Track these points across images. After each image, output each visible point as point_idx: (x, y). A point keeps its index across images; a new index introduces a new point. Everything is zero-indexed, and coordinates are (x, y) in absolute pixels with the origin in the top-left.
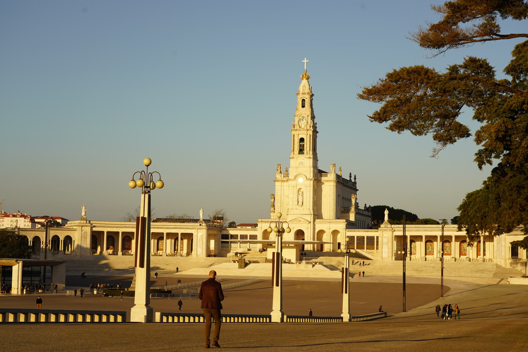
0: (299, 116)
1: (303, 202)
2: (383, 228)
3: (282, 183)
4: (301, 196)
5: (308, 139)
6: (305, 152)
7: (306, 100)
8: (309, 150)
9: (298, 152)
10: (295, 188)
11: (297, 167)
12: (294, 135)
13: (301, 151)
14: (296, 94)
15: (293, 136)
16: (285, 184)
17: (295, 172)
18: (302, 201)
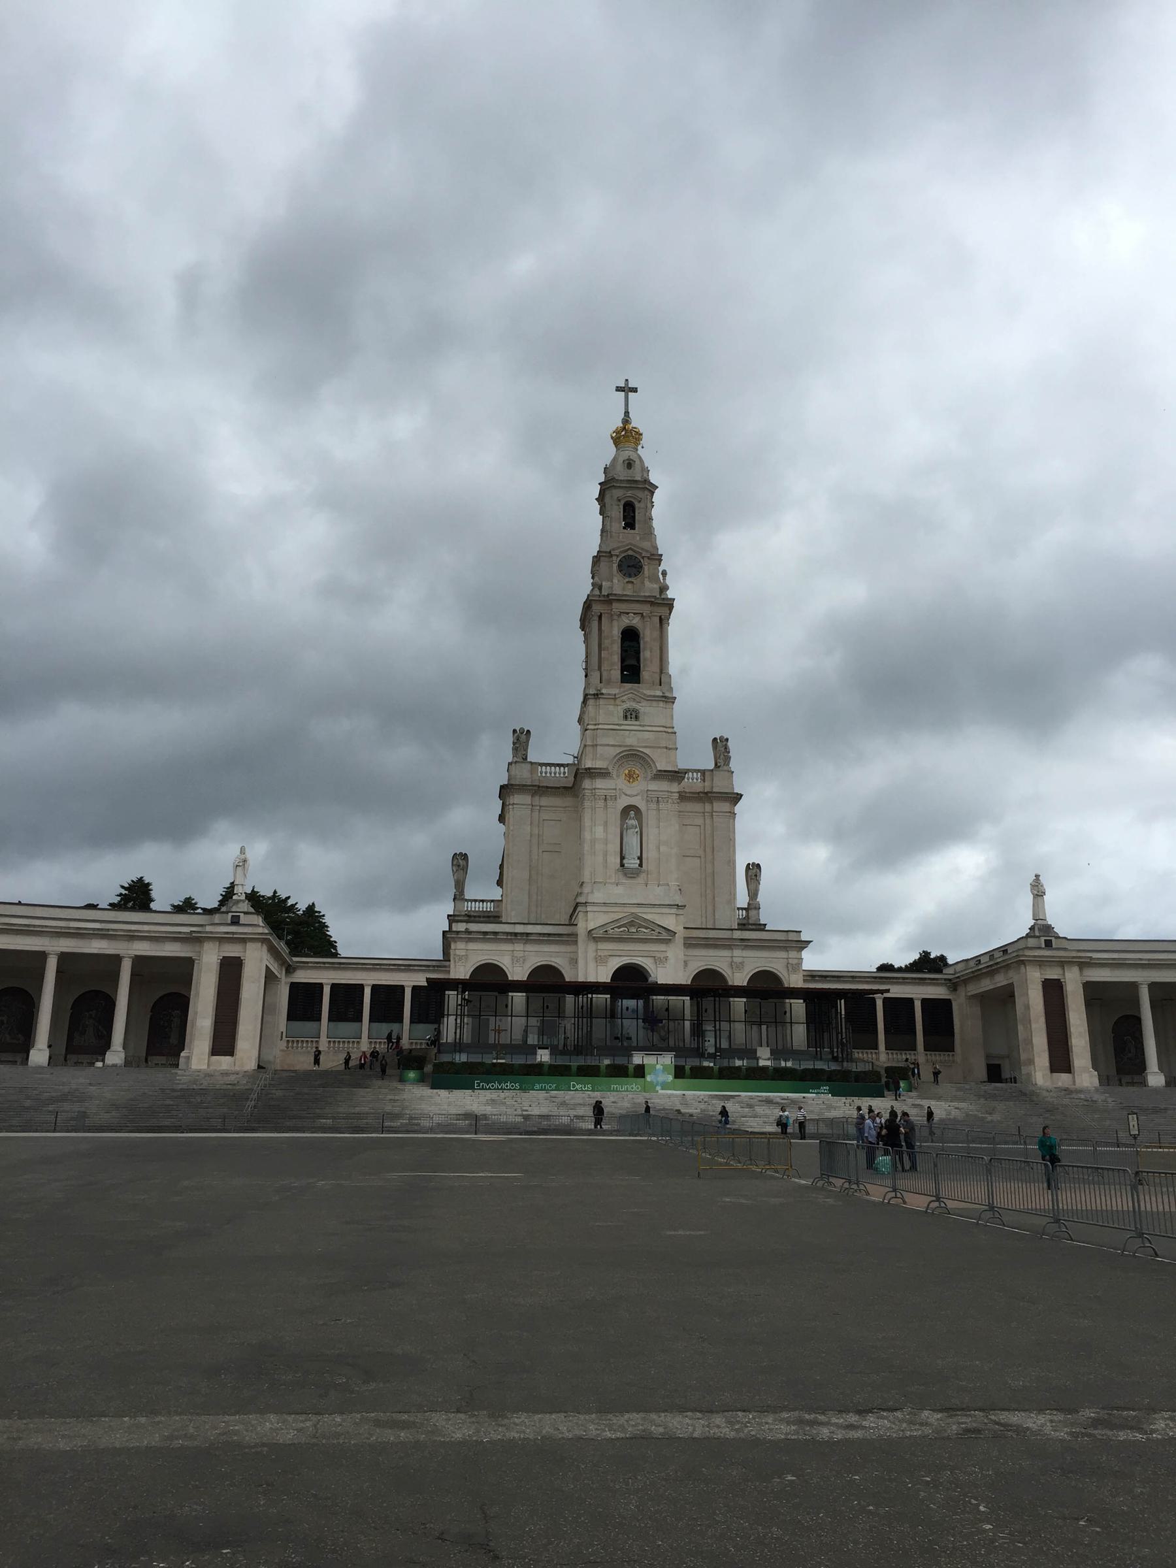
0: (617, 552)
1: (640, 858)
2: (1040, 948)
3: (537, 798)
4: (637, 832)
5: (656, 634)
6: (645, 675)
7: (637, 505)
8: (658, 671)
9: (616, 673)
10: (610, 803)
11: (617, 727)
12: (601, 614)
13: (631, 672)
14: (599, 484)
15: (596, 618)
16: (545, 801)
17: (608, 745)
18: (639, 854)
